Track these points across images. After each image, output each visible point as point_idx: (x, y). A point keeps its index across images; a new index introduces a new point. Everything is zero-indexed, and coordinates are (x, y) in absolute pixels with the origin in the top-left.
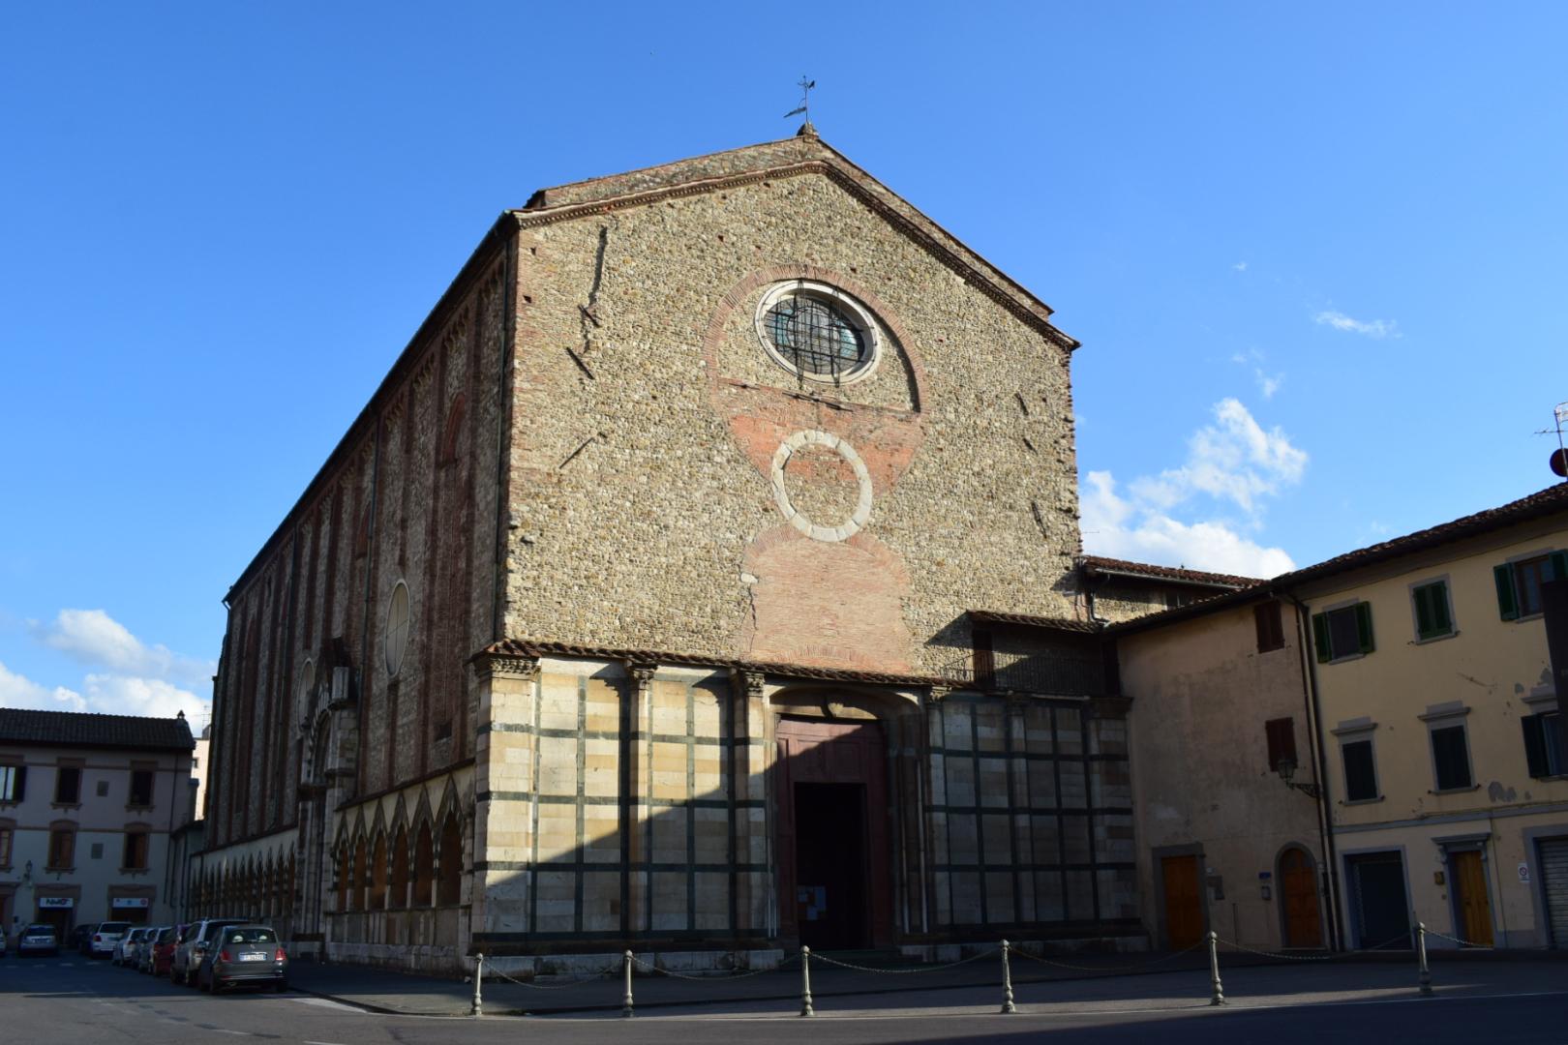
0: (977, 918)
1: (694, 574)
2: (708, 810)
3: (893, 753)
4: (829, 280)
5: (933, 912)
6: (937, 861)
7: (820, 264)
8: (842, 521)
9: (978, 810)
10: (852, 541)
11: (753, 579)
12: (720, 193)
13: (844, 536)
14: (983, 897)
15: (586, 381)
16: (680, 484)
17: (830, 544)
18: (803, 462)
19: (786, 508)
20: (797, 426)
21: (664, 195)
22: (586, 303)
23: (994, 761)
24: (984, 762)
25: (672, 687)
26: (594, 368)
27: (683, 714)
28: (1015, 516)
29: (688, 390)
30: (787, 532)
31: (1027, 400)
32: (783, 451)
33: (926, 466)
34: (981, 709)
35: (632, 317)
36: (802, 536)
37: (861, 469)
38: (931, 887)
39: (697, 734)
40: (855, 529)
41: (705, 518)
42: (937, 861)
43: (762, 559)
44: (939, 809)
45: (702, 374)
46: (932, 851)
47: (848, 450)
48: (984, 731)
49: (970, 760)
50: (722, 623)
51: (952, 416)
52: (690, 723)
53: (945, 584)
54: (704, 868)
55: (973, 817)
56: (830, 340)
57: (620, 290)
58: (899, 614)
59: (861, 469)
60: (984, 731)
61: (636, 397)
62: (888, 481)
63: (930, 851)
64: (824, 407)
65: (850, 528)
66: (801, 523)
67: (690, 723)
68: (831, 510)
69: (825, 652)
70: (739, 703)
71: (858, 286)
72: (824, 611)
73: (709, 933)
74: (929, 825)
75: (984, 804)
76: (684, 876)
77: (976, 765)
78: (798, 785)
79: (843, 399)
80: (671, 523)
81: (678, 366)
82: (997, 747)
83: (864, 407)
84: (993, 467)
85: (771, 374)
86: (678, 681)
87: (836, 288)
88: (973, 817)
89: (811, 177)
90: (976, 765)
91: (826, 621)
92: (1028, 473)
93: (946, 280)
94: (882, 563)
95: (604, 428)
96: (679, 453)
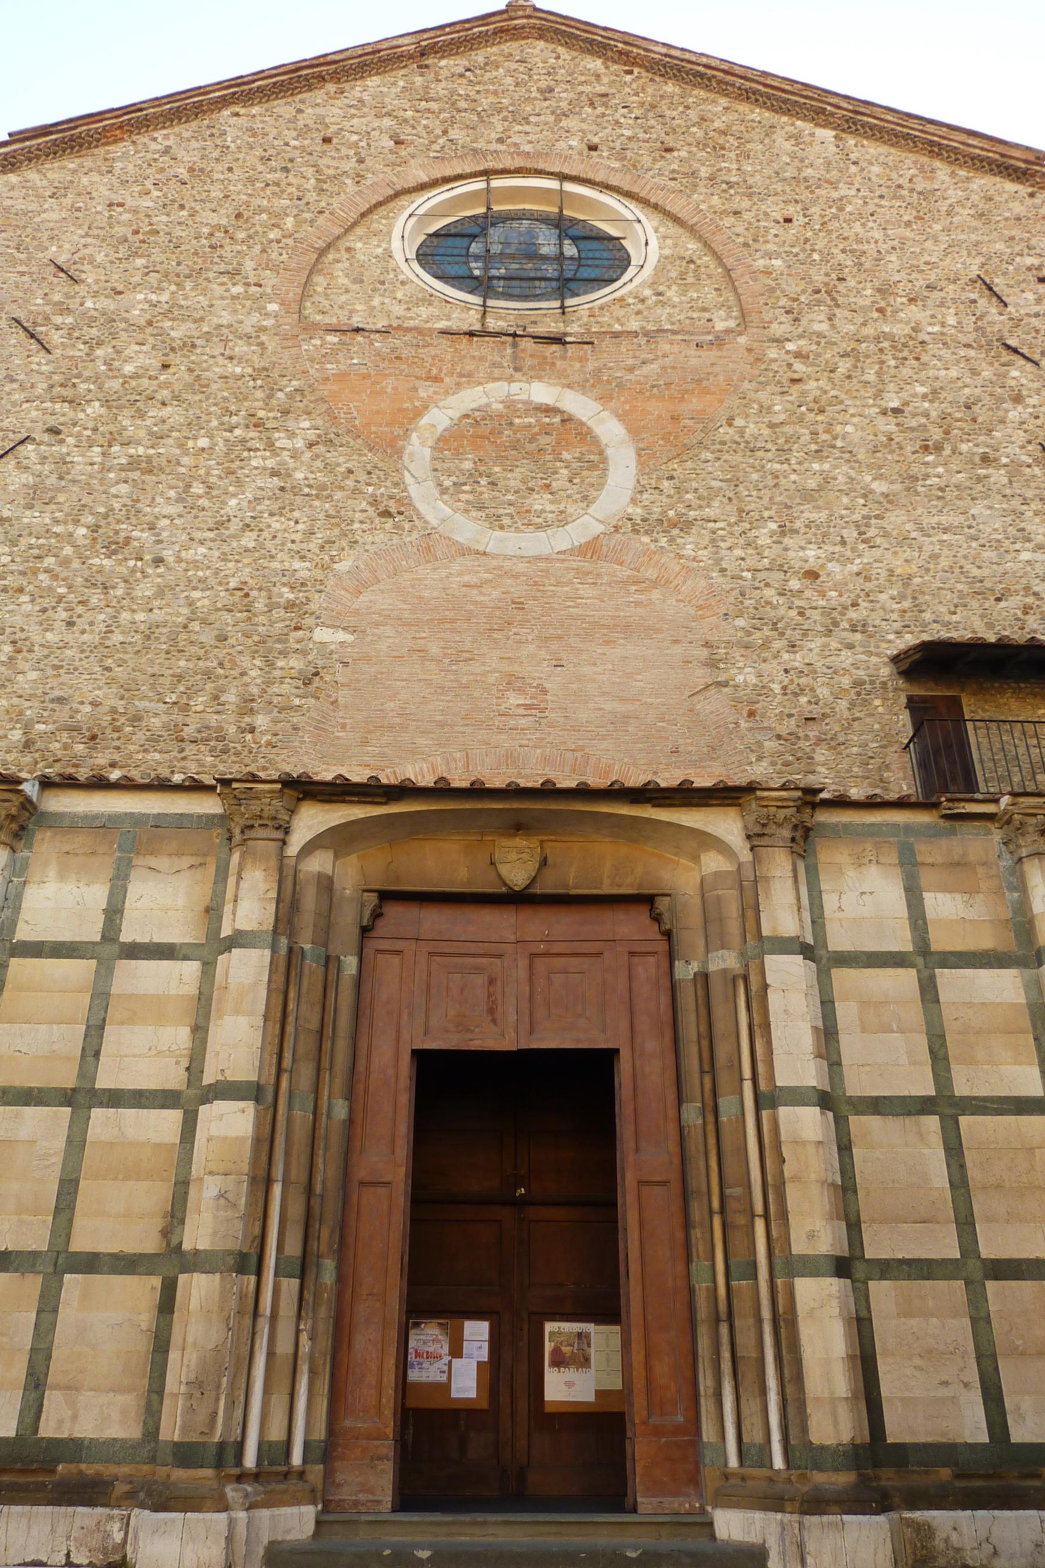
0: (971, 1426)
1: (207, 637)
2: (129, 1115)
3: (686, 971)
4: (541, 165)
5: (794, 1405)
6: (798, 1247)
7: (528, 148)
8: (563, 519)
9: (946, 1106)
10: (591, 549)
11: (349, 638)
12: (331, 87)
13: (565, 546)
14: (987, 1360)
15: (41, 357)
16: (198, 489)
17: (539, 558)
18: (483, 438)
19: (431, 506)
20: (468, 378)
21: (224, 102)
22: (61, 260)
23: (985, 976)
24: (951, 982)
25: (80, 841)
26: (56, 338)
27: (98, 895)
28: (998, 477)
29: (240, 348)
30: (431, 545)
31: (999, 283)
32: (439, 418)
33: (765, 409)
34: (929, 852)
35: (140, 262)
36: (465, 551)
37: (609, 429)
38: (786, 1324)
39: (126, 936)
40: (600, 528)
41: (248, 540)
42: (798, 1247)
43: (365, 598)
44: (797, 1097)
45: (268, 323)
46: (784, 1215)
47: (579, 405)
48: (942, 906)
49: (906, 980)
50: (261, 721)
51: (824, 327)
52: (114, 913)
53: (828, 611)
54: (90, 1263)
55: (932, 1123)
56: (560, 257)
57: (127, 232)
58: (701, 676)
59: (609, 429)
60: (942, 906)
61: (128, 369)
62: (670, 442)
63: (777, 1215)
64: (527, 344)
65: (586, 526)
66: (467, 529)
67: (114, 913)
68: (540, 502)
69: (510, 757)
70: (236, 857)
71: (605, 166)
72: (512, 682)
73: (73, 1449)
74: (772, 1147)
75: (962, 1088)
76: (33, 1284)
77: (929, 990)
78: (420, 1056)
79: (574, 328)
80: (168, 555)
81: (226, 318)
82: (985, 941)
83: (616, 335)
84: (934, 395)
85: (424, 311)
86: (103, 826)
87: (563, 177)
88: (932, 1123)
89: (511, 47)
90: (929, 990)
91: (514, 700)
92: (1018, 399)
93: (796, 138)
94: (655, 584)
95: (52, 422)
96: (203, 442)
